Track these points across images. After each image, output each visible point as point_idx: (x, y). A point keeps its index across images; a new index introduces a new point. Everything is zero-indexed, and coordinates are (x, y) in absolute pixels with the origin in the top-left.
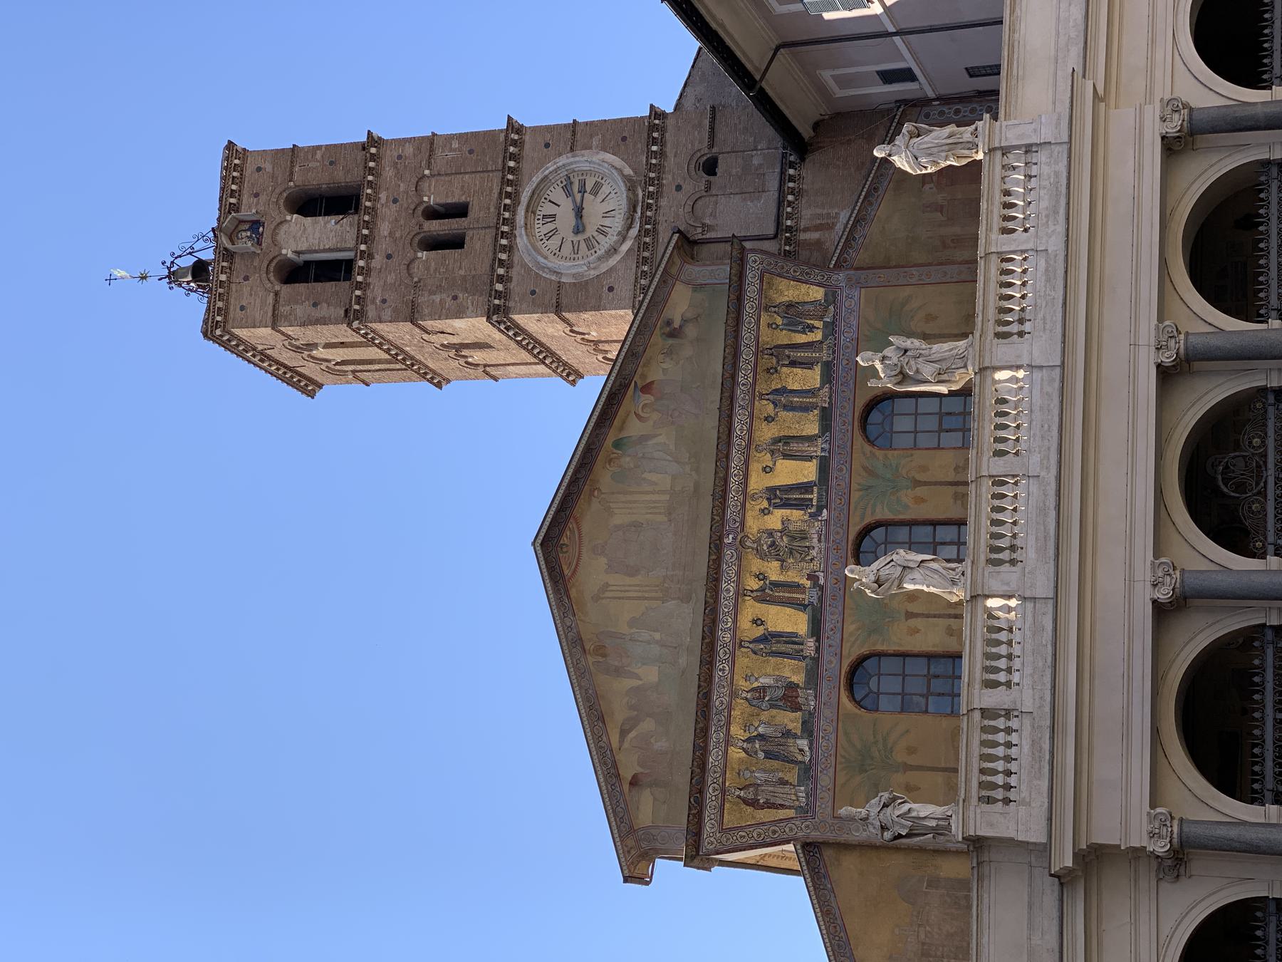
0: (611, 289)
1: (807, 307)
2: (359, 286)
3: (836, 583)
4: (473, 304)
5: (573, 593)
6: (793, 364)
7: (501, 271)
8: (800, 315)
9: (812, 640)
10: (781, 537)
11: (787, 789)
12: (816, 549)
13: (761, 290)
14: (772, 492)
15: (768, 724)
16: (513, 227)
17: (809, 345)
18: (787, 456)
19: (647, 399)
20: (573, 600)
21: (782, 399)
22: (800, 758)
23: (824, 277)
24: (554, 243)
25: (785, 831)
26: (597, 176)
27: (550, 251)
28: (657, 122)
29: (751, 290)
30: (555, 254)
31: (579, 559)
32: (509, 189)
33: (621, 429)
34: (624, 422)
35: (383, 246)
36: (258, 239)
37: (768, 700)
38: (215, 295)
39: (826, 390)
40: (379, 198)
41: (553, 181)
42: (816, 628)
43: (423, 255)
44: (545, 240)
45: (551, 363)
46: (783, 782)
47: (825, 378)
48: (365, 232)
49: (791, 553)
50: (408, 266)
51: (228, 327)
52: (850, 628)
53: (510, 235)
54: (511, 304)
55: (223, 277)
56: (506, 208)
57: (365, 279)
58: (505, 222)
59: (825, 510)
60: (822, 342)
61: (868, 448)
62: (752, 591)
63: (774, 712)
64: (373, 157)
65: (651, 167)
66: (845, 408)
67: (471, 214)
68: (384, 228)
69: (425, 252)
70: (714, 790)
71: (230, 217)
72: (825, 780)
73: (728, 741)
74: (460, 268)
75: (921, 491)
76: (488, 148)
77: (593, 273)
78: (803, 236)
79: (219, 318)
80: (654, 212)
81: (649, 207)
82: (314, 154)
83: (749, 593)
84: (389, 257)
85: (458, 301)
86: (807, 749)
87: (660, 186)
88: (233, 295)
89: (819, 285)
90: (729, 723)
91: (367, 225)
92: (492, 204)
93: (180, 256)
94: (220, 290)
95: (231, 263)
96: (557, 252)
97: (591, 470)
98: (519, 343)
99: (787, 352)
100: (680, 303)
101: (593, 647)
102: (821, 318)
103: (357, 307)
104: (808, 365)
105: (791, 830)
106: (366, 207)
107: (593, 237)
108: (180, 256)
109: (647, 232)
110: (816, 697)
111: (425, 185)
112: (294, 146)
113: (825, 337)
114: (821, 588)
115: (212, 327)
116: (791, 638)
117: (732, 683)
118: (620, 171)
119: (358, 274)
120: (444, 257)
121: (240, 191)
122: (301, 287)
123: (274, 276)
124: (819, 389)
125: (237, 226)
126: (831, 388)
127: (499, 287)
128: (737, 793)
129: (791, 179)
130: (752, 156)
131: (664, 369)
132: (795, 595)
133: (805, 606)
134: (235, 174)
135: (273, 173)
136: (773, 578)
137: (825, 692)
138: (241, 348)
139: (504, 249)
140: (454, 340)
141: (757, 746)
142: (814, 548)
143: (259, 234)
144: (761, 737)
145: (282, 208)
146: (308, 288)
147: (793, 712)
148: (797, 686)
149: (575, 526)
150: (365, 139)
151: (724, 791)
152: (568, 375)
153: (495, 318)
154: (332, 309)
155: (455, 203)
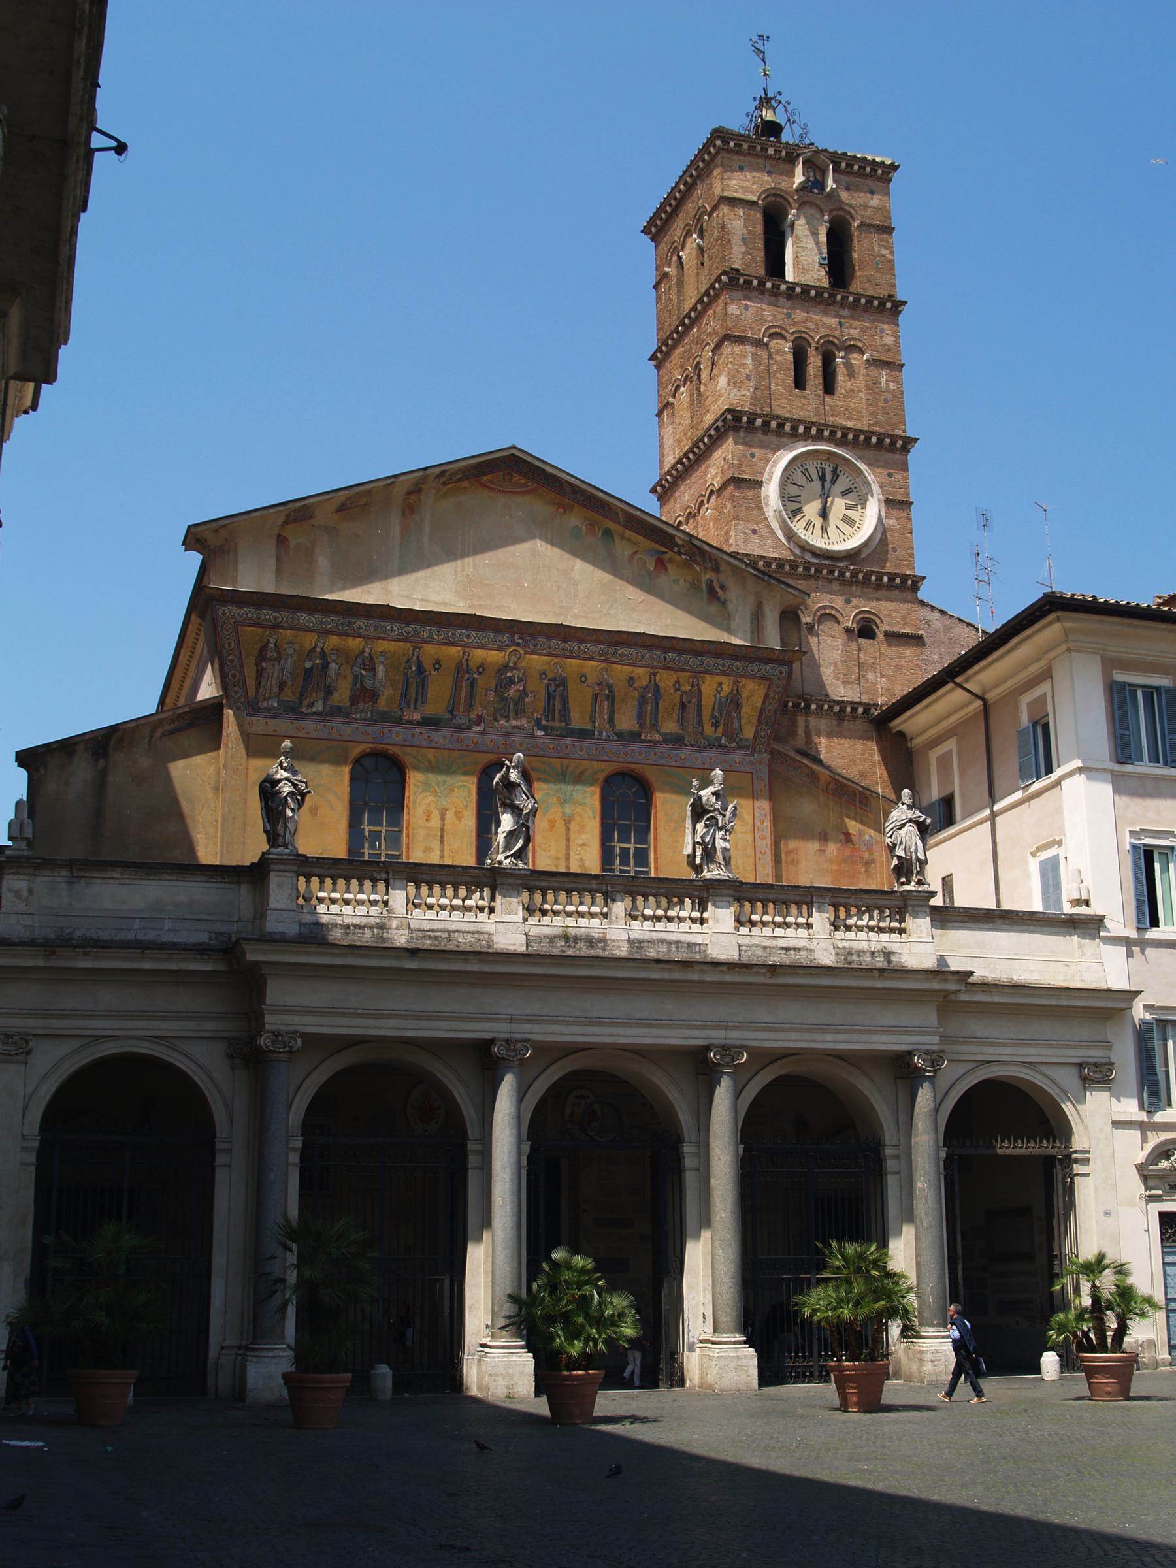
0: (754, 532)
1: (736, 721)
2: (762, 284)
3: (473, 742)
4: (744, 395)
5: (465, 484)
6: (683, 706)
8: (729, 712)
9: (419, 717)
10: (518, 690)
11: (276, 690)
12: (507, 724)
14: (561, 682)
15: (338, 674)
17: (700, 723)
18: (596, 696)
20: (458, 484)
21: (650, 695)
22: (306, 703)
23: (764, 738)
24: (800, 478)
25: (235, 686)
26: (861, 522)
27: (791, 474)
28: (910, 582)
29: (754, 668)
30: (788, 478)
31: (500, 491)
32: (850, 436)
33: (622, 537)
34: (629, 540)
36: (807, 188)
37: (361, 673)
38: (755, 142)
40: (844, 308)
41: (857, 479)
42: (428, 722)
44: (801, 469)
45: (677, 470)
46: (282, 685)
47: (669, 737)
48: (813, 293)
51: (723, 154)
54: (742, 434)
55: (771, 151)
56: (833, 433)
57: (768, 289)
58: (820, 432)
59: (543, 733)
60: (702, 734)
61: (602, 776)
62: (467, 660)
63: (350, 679)
64: (882, 304)
66: (640, 755)
69: (792, 350)
70: (276, 619)
71: (829, 162)
73: (324, 633)
74: (777, 385)
75: (560, 825)
76: (889, 418)
77: (770, 514)
78: (801, 721)
79: (732, 144)
80: (826, 576)
81: (831, 572)
82: (886, 248)
83: (465, 657)
85: (746, 381)
86: (314, 710)
87: (851, 584)
88: (754, 160)
90: (340, 634)
92: (837, 419)
93: (786, 110)
94: (759, 148)
95: (784, 160)
96: (791, 480)
97: (584, 506)
98: (702, 440)
99: (695, 700)
101: (411, 501)
102: (725, 734)
103: (741, 281)
104: (681, 721)
105: (236, 693)
106: (836, 295)
107: (803, 517)
108: (786, 110)
109: (807, 569)
110: (364, 720)
112: (894, 229)
114: (469, 728)
115: (724, 137)
116: (421, 697)
117: (379, 638)
119: (773, 284)
120: (787, 369)
121: (852, 173)
122: (760, 228)
123: (772, 201)
124: (658, 731)
125: (818, 167)
126: (659, 742)
127: (759, 422)
128: (272, 640)
129: (854, 710)
130: (875, 672)
131: (678, 580)
132: (462, 701)
133: (451, 712)
134: (868, 169)
135: (868, 207)
136: (479, 682)
137: (369, 729)
138: (701, 164)
139: (795, 428)
140: (704, 375)
141: (317, 661)
142: (507, 721)
143: (812, 188)
144: (325, 666)
145: (835, 213)
146: (760, 234)
147: (350, 697)
148: (375, 702)
149: (531, 487)
150: (899, 298)
151: (275, 627)
152: (662, 486)
153: (729, 417)
154: (741, 256)
155: (836, 381)
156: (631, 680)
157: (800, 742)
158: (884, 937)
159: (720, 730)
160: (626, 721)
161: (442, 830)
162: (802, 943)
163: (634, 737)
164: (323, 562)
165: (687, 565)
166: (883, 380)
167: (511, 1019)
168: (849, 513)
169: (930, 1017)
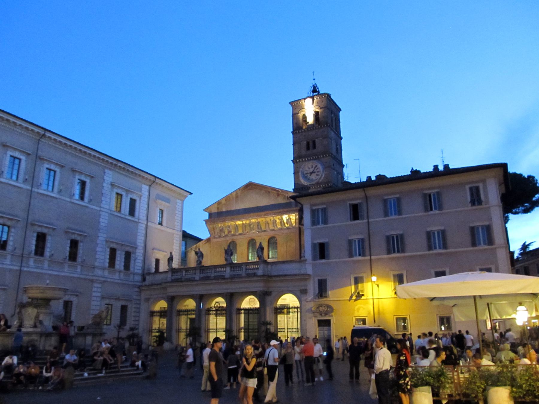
6: (281, 222)
18: (265, 224)
42: (240, 234)
43: (305, 142)
46: (218, 233)
48: (309, 129)
49: (250, 228)
52: (240, 240)
54: (295, 164)
64: (324, 126)
84: (305, 136)
89: (296, 225)
104: (281, 225)
113: (287, 227)
116: (238, 230)
144: (223, 229)
156: (262, 221)
158: (255, 270)
159: (289, 225)
161: (242, 253)
162: (241, 273)
166: (325, 142)
168: (318, 173)
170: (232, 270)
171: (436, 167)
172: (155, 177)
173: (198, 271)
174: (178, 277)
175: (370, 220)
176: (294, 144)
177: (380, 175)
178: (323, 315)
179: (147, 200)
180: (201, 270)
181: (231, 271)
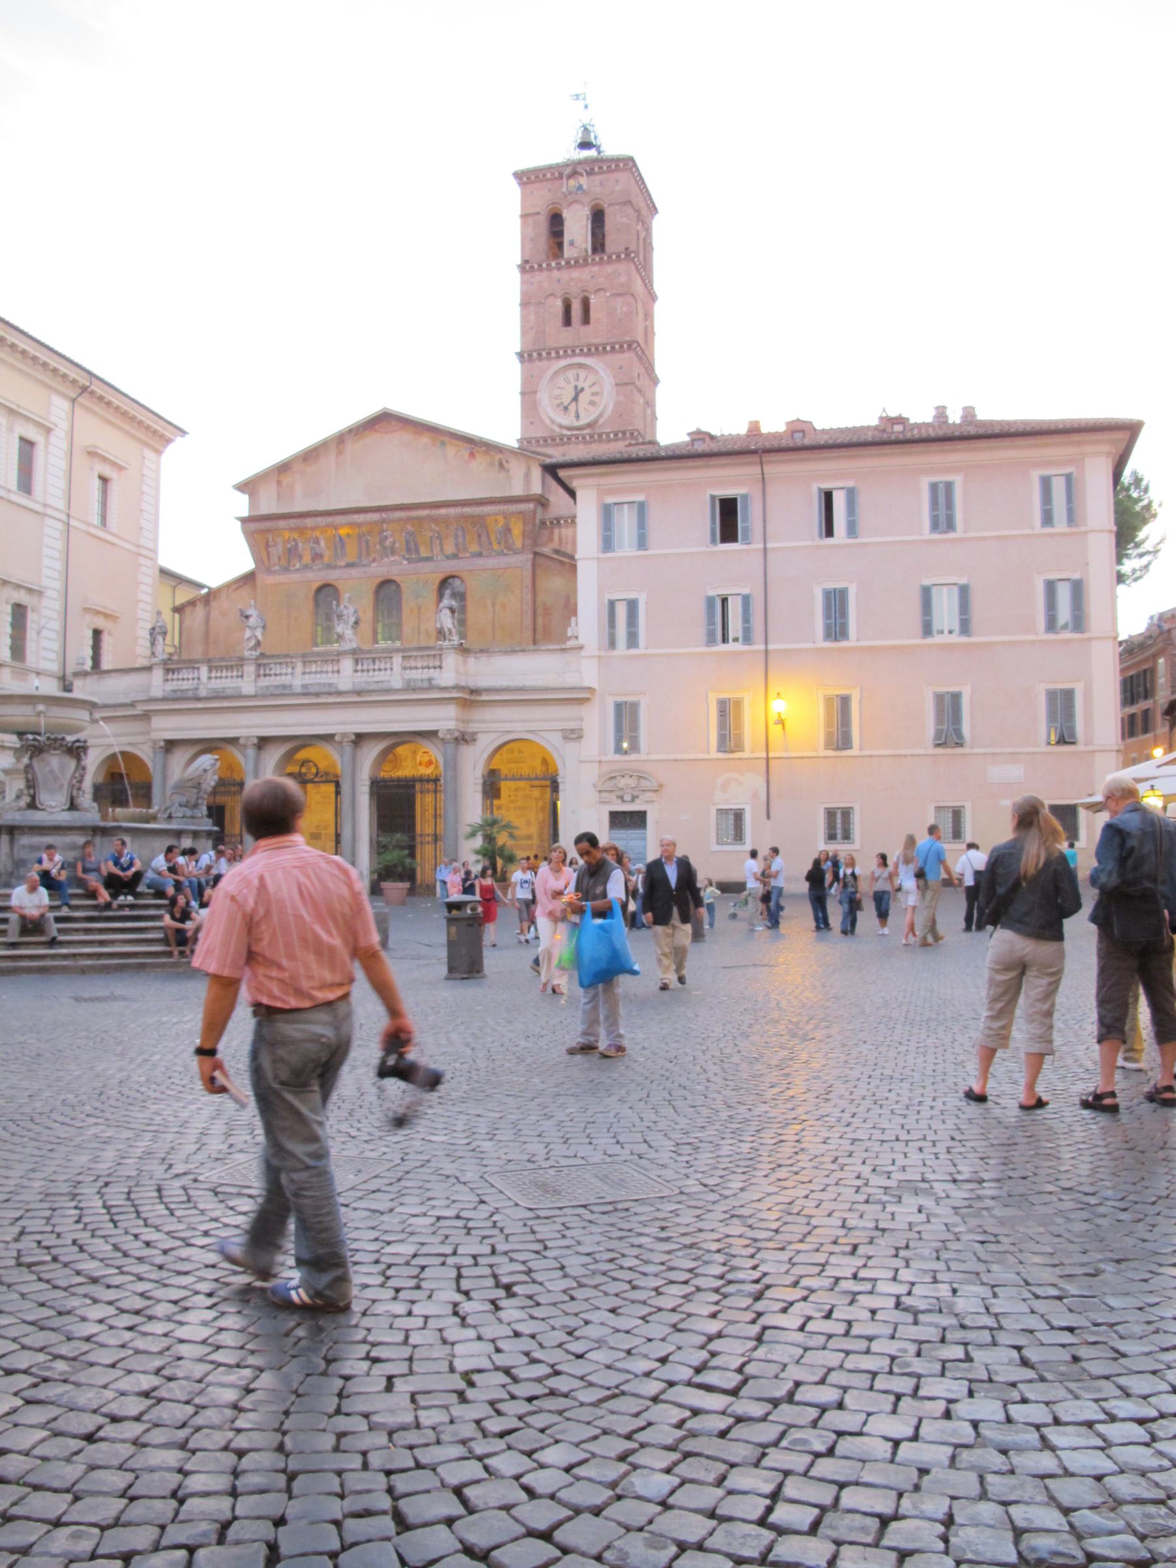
2: (540, 265)
6: (479, 536)
7: (544, 354)
13: (513, 513)
16: (571, 356)
17: (490, 543)
19: (466, 454)
35: (565, 275)
39: (468, 555)
43: (559, 303)
46: (279, 558)
49: (384, 548)
50: (552, 295)
53: (566, 355)
55: (549, 176)
56: (582, 350)
58: (573, 351)
64: (618, 256)
65: (600, 435)
67: (584, 330)
68: (576, 274)
72: (281, 578)
78: (556, 531)
84: (559, 281)
87: (590, 443)
91: (577, 262)
100: (517, 469)
104: (480, 543)
109: (561, 439)
111: (601, 294)
118: (600, 416)
127: (535, 355)
139: (557, 353)
144: (296, 546)
157: (555, 545)
158: (432, 670)
160: (450, 549)
162: (387, 678)
163: (455, 556)
164: (298, 490)
165: (487, 452)
167: (248, 727)
168: (595, 399)
169: (451, 711)
170: (359, 667)
171: (941, 412)
172: (90, 373)
173: (250, 669)
174: (186, 685)
175: (769, 545)
176: (525, 304)
177: (798, 420)
178: (627, 798)
179: (64, 445)
180: (259, 666)
181: (356, 671)
